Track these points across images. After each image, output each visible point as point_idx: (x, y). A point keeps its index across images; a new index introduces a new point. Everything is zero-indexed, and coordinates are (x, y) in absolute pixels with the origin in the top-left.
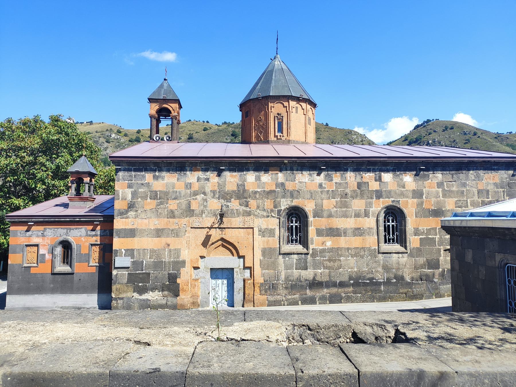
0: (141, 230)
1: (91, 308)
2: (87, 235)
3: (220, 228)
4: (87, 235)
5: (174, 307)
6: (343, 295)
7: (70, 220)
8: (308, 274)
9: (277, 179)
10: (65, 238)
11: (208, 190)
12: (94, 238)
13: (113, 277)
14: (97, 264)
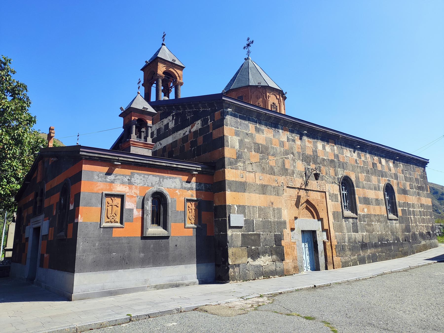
0: (250, 184)
1: (190, 283)
2: (182, 187)
3: (306, 189)
4: (182, 188)
5: (282, 273)
6: (378, 255)
7: (166, 166)
8: (358, 236)
9: (334, 151)
10: (159, 189)
11: (295, 152)
12: (189, 191)
13: (229, 239)
14: (193, 226)
